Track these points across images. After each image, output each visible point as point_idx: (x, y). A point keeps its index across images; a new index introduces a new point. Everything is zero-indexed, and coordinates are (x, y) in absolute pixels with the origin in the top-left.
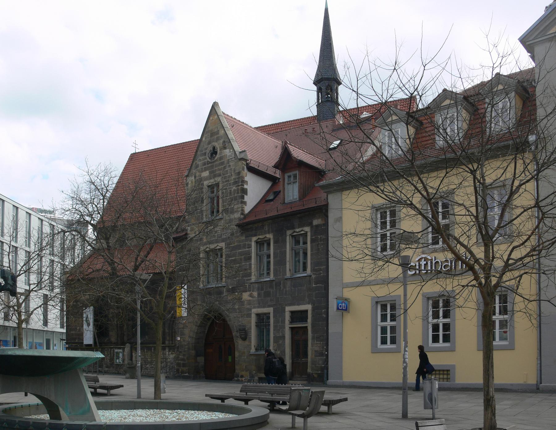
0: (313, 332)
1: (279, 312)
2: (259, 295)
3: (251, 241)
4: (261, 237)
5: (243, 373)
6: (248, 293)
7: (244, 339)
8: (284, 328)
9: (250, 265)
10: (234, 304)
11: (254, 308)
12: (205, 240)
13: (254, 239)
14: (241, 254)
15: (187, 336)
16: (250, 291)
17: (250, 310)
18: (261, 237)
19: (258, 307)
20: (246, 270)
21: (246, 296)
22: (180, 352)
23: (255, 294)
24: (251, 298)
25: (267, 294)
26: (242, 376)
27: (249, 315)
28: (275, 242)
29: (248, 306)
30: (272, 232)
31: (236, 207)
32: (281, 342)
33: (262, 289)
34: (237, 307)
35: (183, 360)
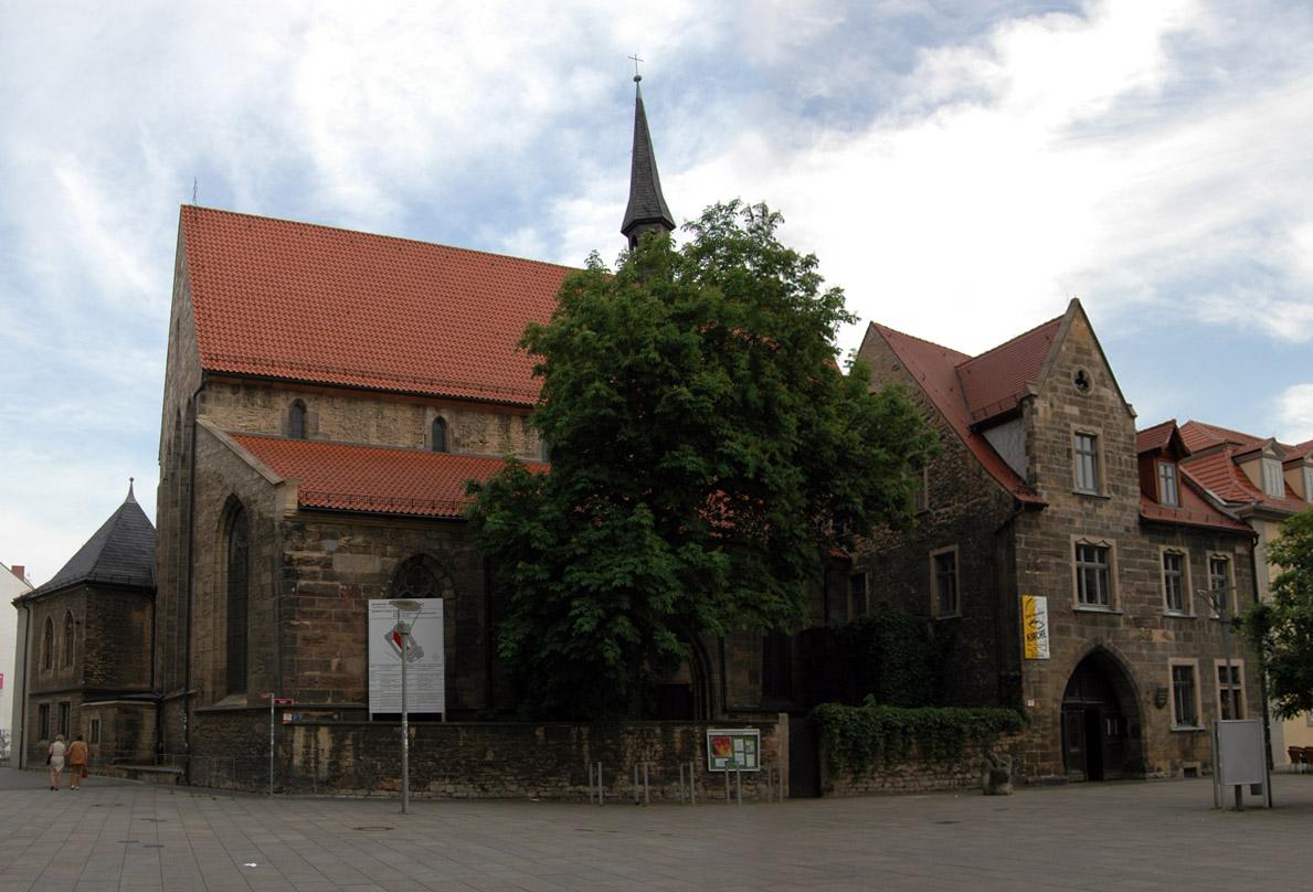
0: (1249, 698)
1: (1206, 664)
2: (1177, 635)
3: (1158, 549)
4: (1173, 548)
5: (1161, 764)
6: (1161, 631)
7: (1159, 706)
8: (1214, 690)
9: (1160, 586)
10: (1140, 647)
11: (1172, 656)
12: (1077, 525)
13: (1163, 548)
14: (1144, 566)
15: (1045, 698)
16: (1163, 628)
17: (1166, 659)
18: (1173, 548)
19: (1178, 656)
20: (1153, 593)
21: (1157, 635)
22: (1036, 731)
23: (1171, 634)
24: (1165, 640)
25: (1188, 637)
26: (1159, 770)
27: (1165, 668)
28: (1193, 562)
29: (1161, 652)
30: (1188, 546)
31: (1130, 488)
32: (1212, 711)
33: (1181, 629)
34: (1144, 652)
35: (1042, 746)
